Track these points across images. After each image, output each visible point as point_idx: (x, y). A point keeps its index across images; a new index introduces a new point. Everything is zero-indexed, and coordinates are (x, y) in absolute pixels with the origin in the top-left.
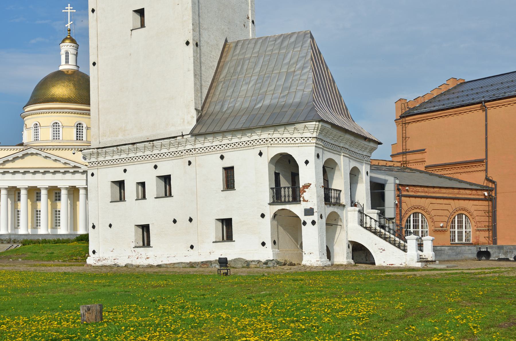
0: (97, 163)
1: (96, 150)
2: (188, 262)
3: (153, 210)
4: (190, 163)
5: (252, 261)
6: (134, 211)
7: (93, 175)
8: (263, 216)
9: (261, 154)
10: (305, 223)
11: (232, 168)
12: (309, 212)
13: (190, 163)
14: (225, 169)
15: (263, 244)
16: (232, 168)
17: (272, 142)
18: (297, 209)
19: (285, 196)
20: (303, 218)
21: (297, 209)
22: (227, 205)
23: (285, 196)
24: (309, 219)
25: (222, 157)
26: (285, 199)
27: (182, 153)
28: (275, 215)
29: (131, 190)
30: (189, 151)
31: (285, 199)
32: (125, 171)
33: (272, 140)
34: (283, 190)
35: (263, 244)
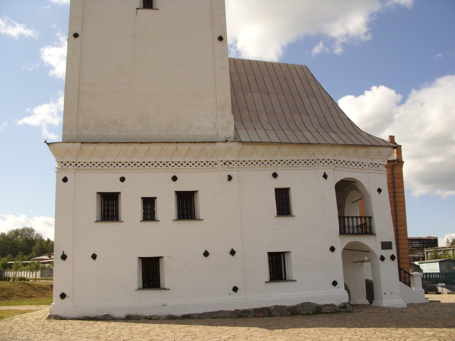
0: (73, 164)
1: (79, 145)
2: (233, 309)
3: (166, 237)
4: (230, 178)
5: (325, 305)
6: (132, 238)
9: (325, 176)
10: (382, 258)
12: (386, 246)
13: (230, 178)
15: (335, 283)
17: (336, 165)
18: (372, 243)
19: (353, 227)
20: (379, 252)
21: (372, 243)
22: (278, 234)
23: (349, 226)
24: (387, 253)
26: (349, 231)
27: (216, 164)
28: (346, 249)
29: (130, 208)
30: (228, 163)
31: (349, 231)
32: (122, 179)
33: (337, 163)
34: (346, 219)
35: (335, 283)
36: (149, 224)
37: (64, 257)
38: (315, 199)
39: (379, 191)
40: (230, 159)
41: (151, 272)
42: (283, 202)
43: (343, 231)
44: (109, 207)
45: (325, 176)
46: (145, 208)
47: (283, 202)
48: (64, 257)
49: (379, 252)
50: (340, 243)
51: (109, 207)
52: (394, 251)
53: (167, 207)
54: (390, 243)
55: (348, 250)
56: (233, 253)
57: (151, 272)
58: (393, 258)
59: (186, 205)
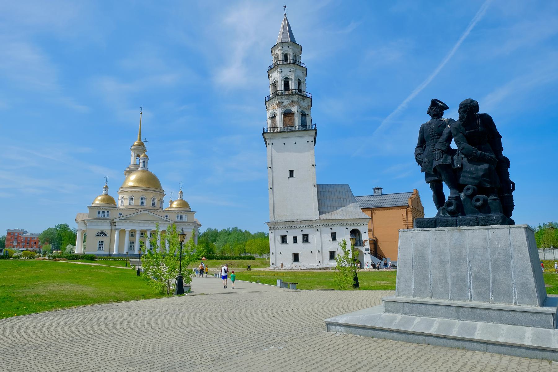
3: (300, 248)
6: (291, 248)
11: (335, 233)
12: (367, 250)
14: (332, 233)
16: (335, 233)
18: (363, 249)
20: (364, 251)
21: (363, 249)
24: (367, 252)
25: (331, 229)
29: (290, 239)
36: (295, 244)
38: (345, 236)
41: (296, 257)
44: (284, 240)
47: (334, 237)
51: (284, 240)
52: (369, 251)
53: (300, 239)
57: (296, 257)
59: (306, 239)
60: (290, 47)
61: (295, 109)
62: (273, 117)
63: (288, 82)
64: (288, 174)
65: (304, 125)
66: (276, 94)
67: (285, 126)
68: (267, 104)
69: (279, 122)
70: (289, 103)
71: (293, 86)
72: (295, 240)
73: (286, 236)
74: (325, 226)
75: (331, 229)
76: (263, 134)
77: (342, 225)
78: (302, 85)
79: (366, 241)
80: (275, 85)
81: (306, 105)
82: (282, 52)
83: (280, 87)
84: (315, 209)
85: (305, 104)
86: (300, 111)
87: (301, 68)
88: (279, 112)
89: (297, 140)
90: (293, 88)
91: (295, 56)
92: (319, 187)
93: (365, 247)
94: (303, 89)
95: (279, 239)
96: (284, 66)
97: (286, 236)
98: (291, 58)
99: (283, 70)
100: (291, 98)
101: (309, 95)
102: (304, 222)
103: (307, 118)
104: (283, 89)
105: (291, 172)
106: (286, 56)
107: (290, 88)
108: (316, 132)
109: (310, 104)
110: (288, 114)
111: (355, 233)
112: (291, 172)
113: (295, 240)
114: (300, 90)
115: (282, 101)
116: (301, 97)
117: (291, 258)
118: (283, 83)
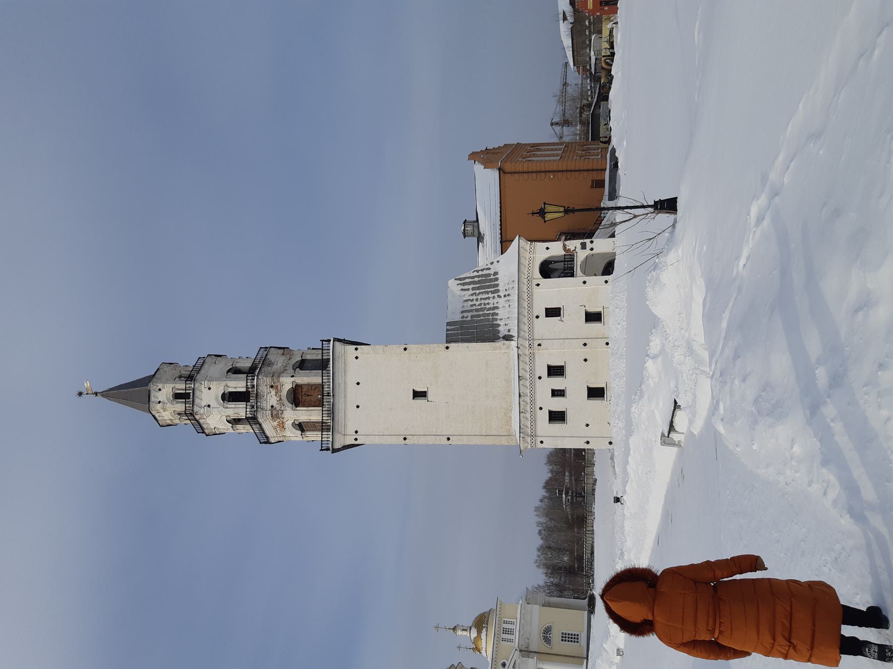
3: (575, 384)
4: (539, 345)
6: (575, 402)
7: (542, 442)
8: (585, 282)
9: (538, 285)
10: (592, 249)
12: (584, 246)
13: (539, 345)
18: (581, 256)
20: (587, 252)
22: (573, 318)
24: (589, 245)
25: (537, 317)
29: (557, 404)
32: (541, 408)
36: (568, 393)
37: (588, 443)
38: (554, 291)
39: (547, 248)
40: (527, 345)
41: (596, 393)
42: (553, 313)
43: (572, 275)
44: (557, 417)
45: (538, 285)
46: (558, 396)
47: (553, 313)
48: (588, 443)
49: (587, 252)
50: (580, 277)
51: (557, 417)
52: (588, 241)
53: (557, 383)
54: (582, 244)
55: (585, 273)
56: (585, 345)
57: (596, 393)
58: (592, 242)
59: (556, 371)
60: (160, 386)
61: (287, 383)
62: (301, 427)
63: (230, 393)
64: (420, 402)
65: (322, 365)
66: (252, 420)
67: (320, 404)
68: (272, 440)
69: (313, 415)
70: (273, 392)
71: (238, 385)
72: (557, 393)
73: (550, 412)
74: (531, 329)
75: (537, 317)
76: (335, 451)
77: (530, 296)
78: (239, 365)
79: (564, 246)
80: (235, 422)
81: (283, 358)
82: (169, 405)
83: (240, 410)
84: (495, 349)
85: (278, 361)
86: (291, 371)
87: (206, 366)
88: (292, 415)
89: (351, 381)
90: (243, 384)
91: (180, 377)
92: (451, 339)
93: (579, 249)
94: (248, 364)
95: (557, 427)
96: (197, 401)
97: (550, 412)
98: (183, 386)
99: (204, 403)
100: (264, 389)
101: (263, 353)
102: (521, 371)
103: (308, 357)
104: (242, 405)
105: (418, 395)
106: (177, 396)
107: (244, 390)
108: (339, 340)
109: (281, 351)
110: (297, 397)
111: (547, 270)
112: (418, 395)
113: (557, 393)
114: (251, 371)
115: (269, 407)
116: (265, 369)
117: (596, 403)
118: (232, 405)
